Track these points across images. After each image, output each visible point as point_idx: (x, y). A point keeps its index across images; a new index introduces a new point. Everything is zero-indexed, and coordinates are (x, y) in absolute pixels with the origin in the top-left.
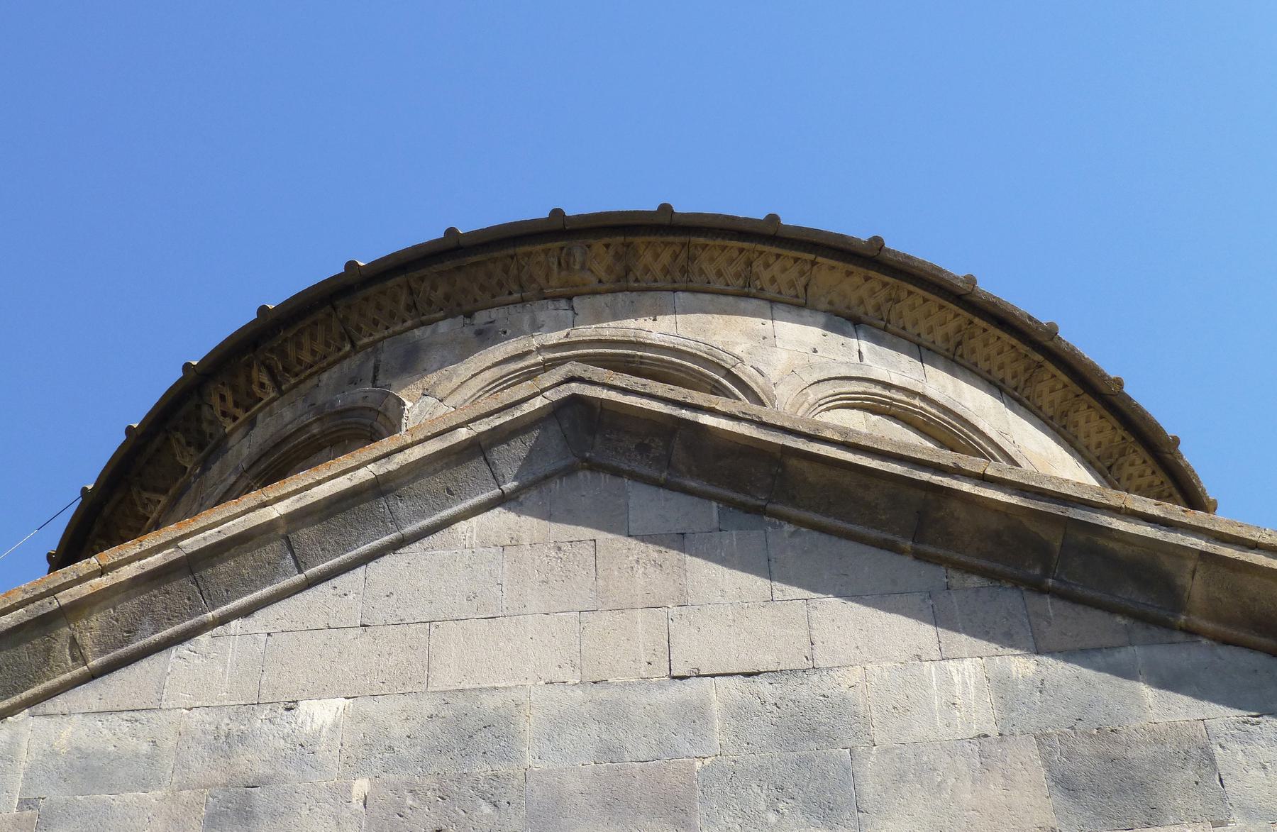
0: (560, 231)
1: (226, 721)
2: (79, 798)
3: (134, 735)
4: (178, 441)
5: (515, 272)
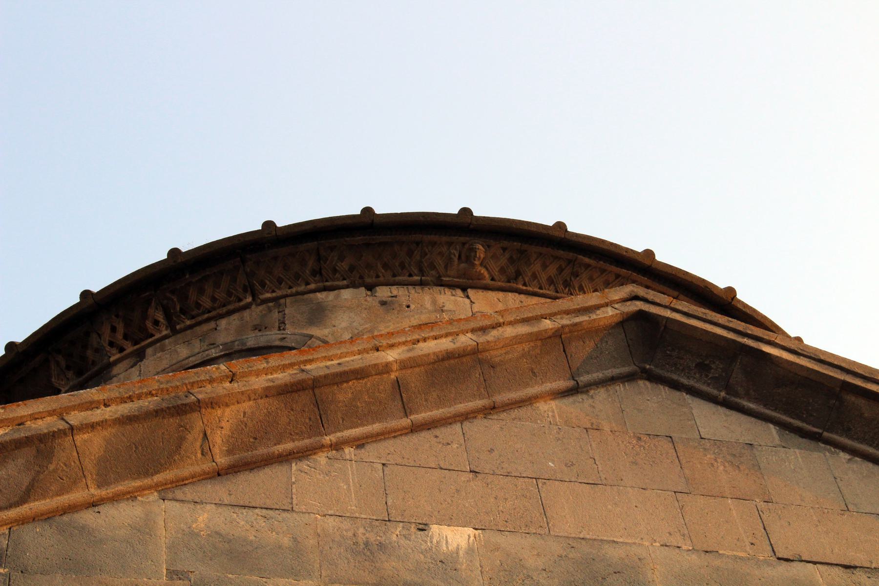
0: (464, 228)
1: (361, 530)
2: (230, 576)
3: (272, 530)
4: (58, 363)
5: (418, 257)
